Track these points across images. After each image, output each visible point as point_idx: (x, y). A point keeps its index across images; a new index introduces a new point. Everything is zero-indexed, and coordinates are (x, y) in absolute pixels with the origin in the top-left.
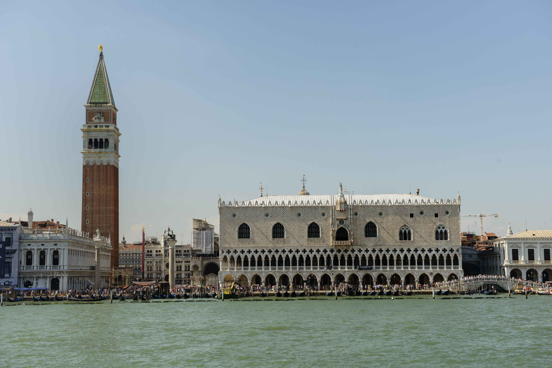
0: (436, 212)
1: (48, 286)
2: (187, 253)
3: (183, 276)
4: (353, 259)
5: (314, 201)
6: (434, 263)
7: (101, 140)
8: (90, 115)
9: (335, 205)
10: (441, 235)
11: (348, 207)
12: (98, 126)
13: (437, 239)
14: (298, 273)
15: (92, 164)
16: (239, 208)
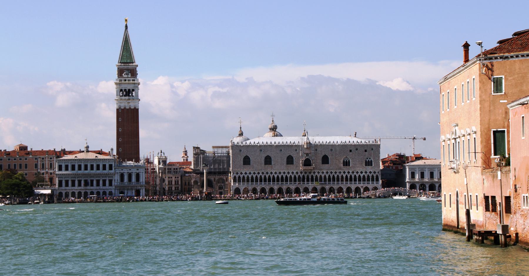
0: (366, 149)
1: (134, 194)
2: (175, 170)
3: (173, 189)
4: (314, 178)
5: (290, 142)
6: (364, 180)
7: (129, 90)
8: (120, 72)
9: (303, 144)
10: (369, 163)
11: (311, 146)
12: (127, 80)
13: (366, 165)
14: (280, 186)
15: (123, 108)
16: (243, 146)
